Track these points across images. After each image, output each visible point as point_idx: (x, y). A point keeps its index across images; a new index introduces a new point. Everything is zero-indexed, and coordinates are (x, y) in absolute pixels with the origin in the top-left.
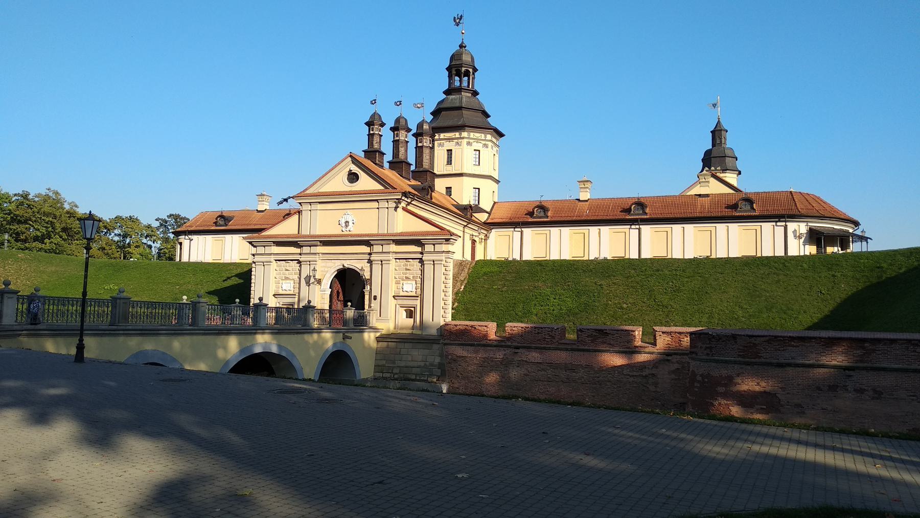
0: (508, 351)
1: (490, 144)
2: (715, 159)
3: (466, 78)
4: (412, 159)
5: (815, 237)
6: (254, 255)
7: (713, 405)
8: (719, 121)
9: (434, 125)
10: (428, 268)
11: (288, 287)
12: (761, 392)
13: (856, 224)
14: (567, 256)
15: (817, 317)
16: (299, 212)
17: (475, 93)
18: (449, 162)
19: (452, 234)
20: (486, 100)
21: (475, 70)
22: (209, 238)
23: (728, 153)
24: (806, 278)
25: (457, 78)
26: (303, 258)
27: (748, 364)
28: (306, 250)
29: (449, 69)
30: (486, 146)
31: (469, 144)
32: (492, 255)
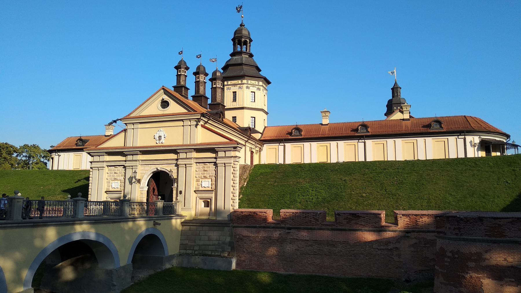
0: (282, 231)
1: (262, 88)
2: (392, 106)
3: (245, 46)
4: (208, 94)
5: (485, 145)
6: (91, 162)
7: (464, 277)
8: (396, 83)
9: (224, 75)
10: (221, 169)
11: (116, 185)
12: (508, 267)
13: (508, 136)
14: (315, 161)
15: (508, 201)
16: (125, 130)
17: (251, 56)
18: (235, 100)
19: (238, 143)
20: (257, 60)
21: (251, 40)
22: (72, 154)
23: (402, 101)
24: (493, 172)
25: (238, 46)
26: (127, 164)
27: (495, 242)
28: (129, 158)
29: (233, 40)
30: (259, 89)
31: (247, 87)
32: (265, 161)
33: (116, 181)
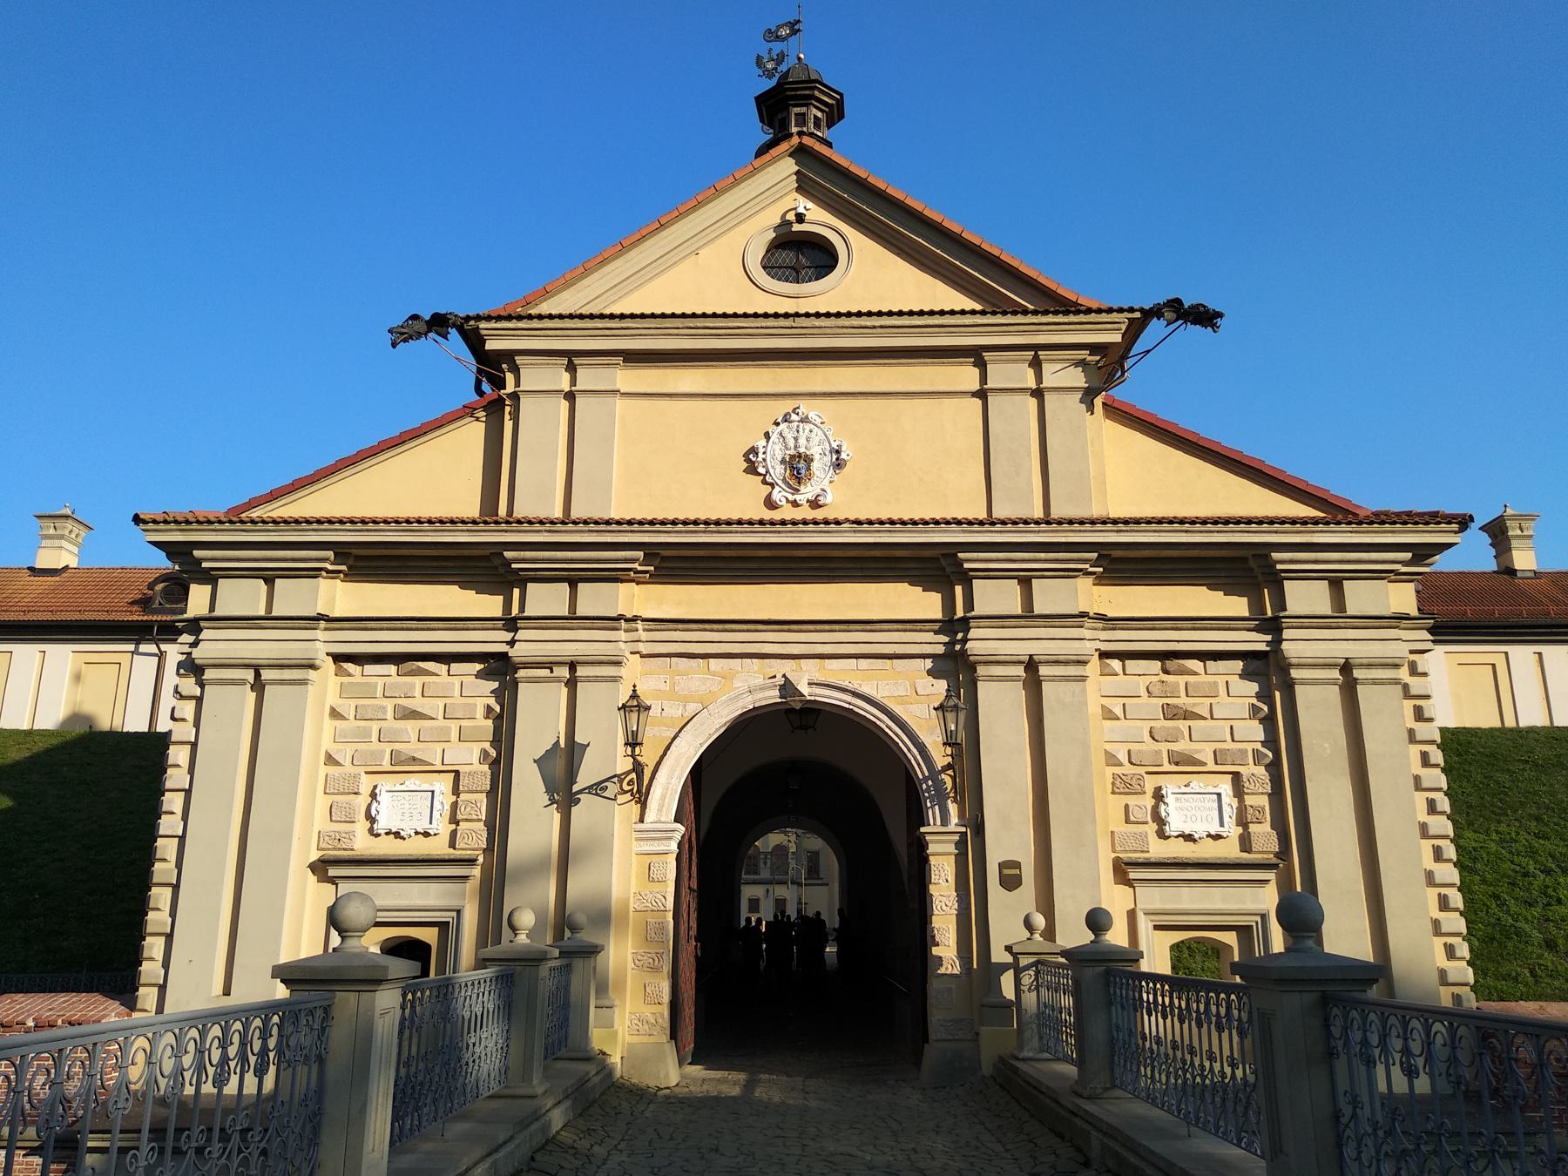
10: (1318, 708)
11: (412, 813)
26: (527, 646)
28: (545, 599)
33: (413, 782)
